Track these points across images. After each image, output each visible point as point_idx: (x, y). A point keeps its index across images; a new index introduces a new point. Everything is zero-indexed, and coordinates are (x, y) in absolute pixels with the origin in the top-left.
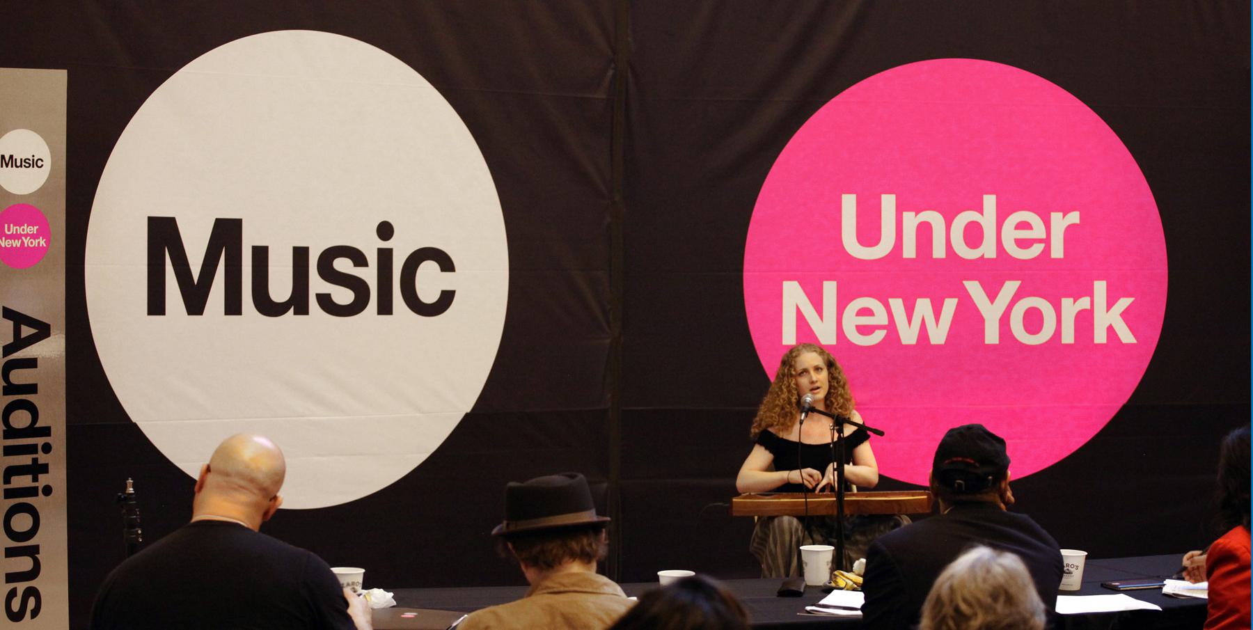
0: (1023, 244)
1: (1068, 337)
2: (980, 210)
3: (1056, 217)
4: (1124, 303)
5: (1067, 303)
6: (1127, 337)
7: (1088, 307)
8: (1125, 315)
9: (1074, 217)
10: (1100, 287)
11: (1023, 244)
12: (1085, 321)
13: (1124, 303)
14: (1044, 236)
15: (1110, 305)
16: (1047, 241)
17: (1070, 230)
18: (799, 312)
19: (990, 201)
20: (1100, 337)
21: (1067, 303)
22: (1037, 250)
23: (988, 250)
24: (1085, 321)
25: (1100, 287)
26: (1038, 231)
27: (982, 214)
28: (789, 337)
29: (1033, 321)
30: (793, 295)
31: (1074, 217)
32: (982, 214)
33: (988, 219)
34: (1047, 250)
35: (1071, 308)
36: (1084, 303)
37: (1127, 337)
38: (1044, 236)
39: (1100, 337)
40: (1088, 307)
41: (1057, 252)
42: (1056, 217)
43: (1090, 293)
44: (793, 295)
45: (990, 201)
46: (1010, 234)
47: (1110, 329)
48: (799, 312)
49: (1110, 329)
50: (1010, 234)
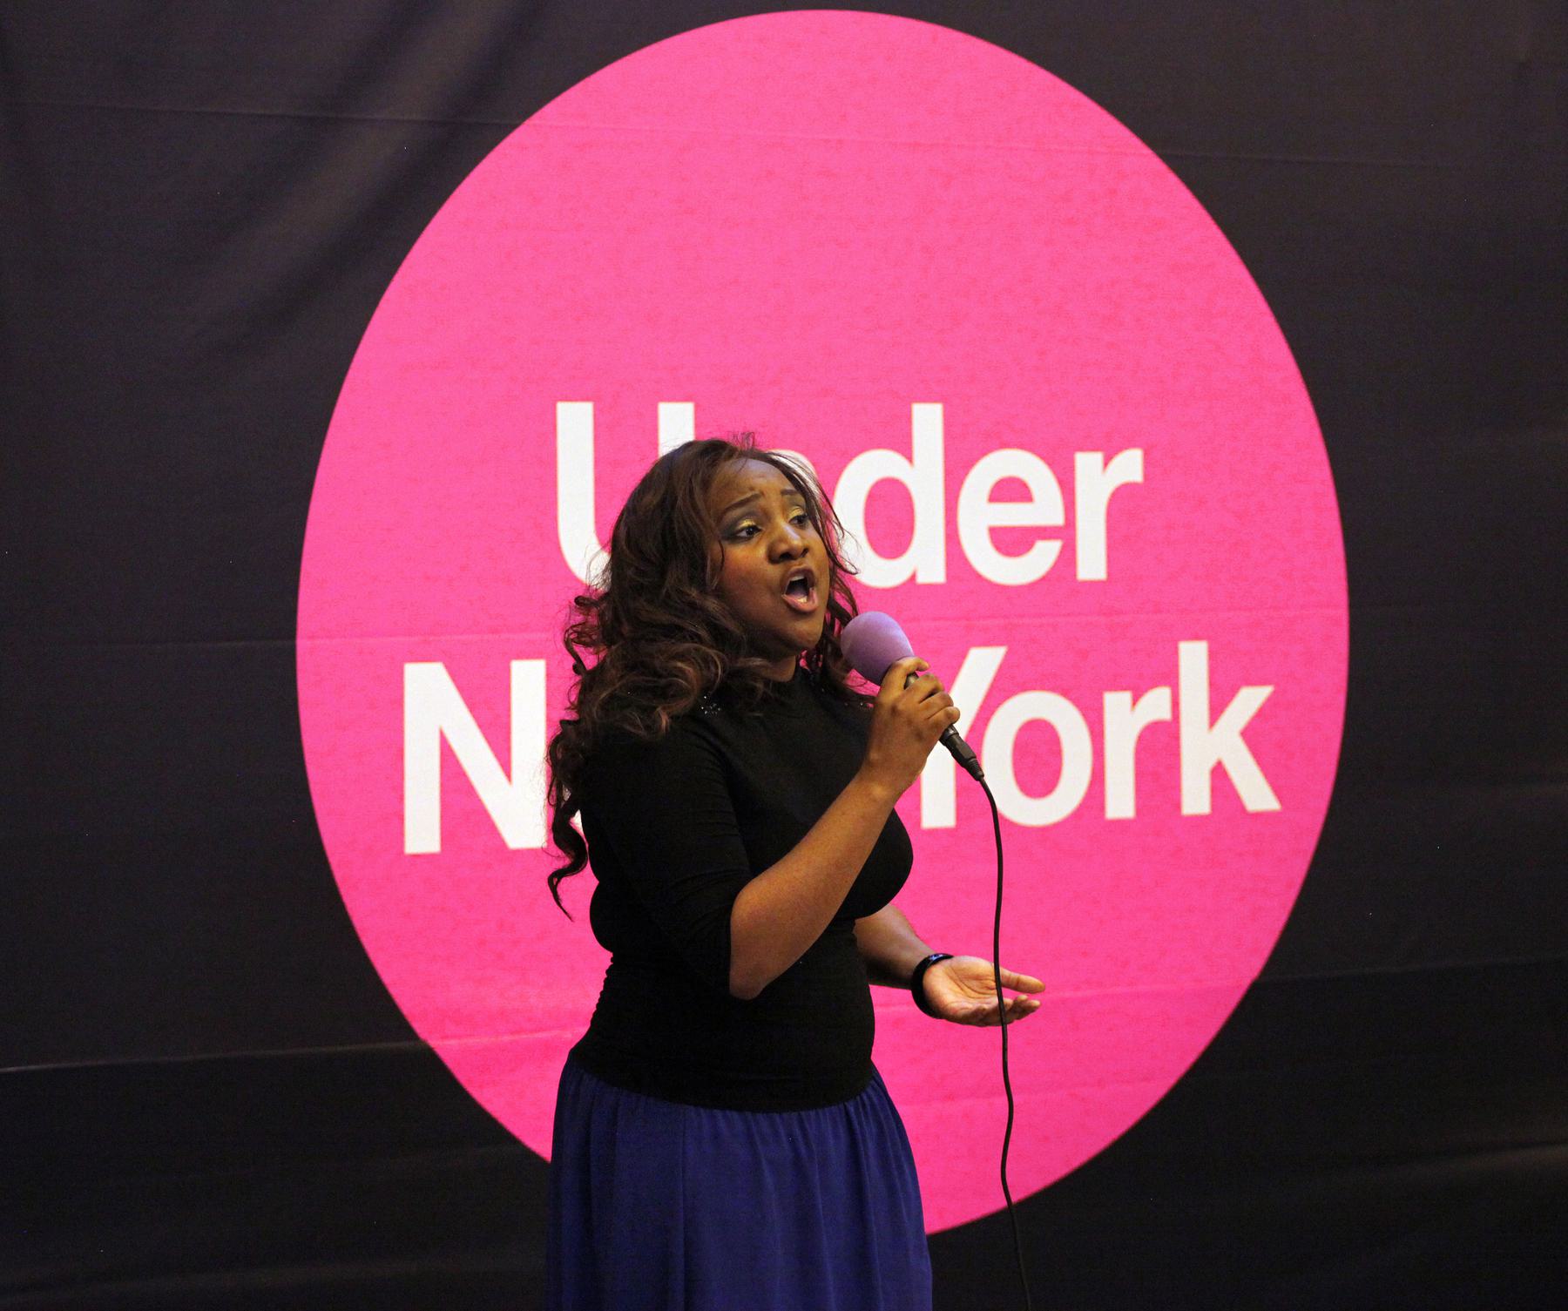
0: (1011, 541)
1: (1121, 803)
2: (908, 455)
3: (1087, 463)
4: (1250, 700)
5: (1115, 703)
6: (1257, 794)
7: (1166, 714)
8: (1252, 735)
9: (1130, 466)
10: (1193, 657)
11: (1011, 541)
12: (1159, 751)
13: (1250, 700)
14: (1058, 519)
15: (1217, 709)
16: (1066, 533)
17: (1122, 503)
18: (447, 755)
19: (928, 420)
20: (1196, 799)
21: (1115, 703)
22: (1044, 555)
23: (924, 561)
24: (1159, 751)
25: (1193, 657)
26: (1045, 508)
27: (910, 458)
28: (422, 832)
29: (1038, 758)
30: (431, 699)
31: (1130, 466)
32: (910, 458)
33: (923, 474)
34: (1068, 557)
35: (1126, 717)
36: (1156, 704)
37: (1257, 794)
38: (1058, 519)
39: (1196, 799)
40: (1166, 714)
41: (1092, 564)
42: (1087, 463)
43: (1170, 677)
44: (431, 699)
45: (928, 420)
46: (979, 515)
47: (1219, 775)
48: (447, 755)
49: (1219, 775)
50: (979, 515)
